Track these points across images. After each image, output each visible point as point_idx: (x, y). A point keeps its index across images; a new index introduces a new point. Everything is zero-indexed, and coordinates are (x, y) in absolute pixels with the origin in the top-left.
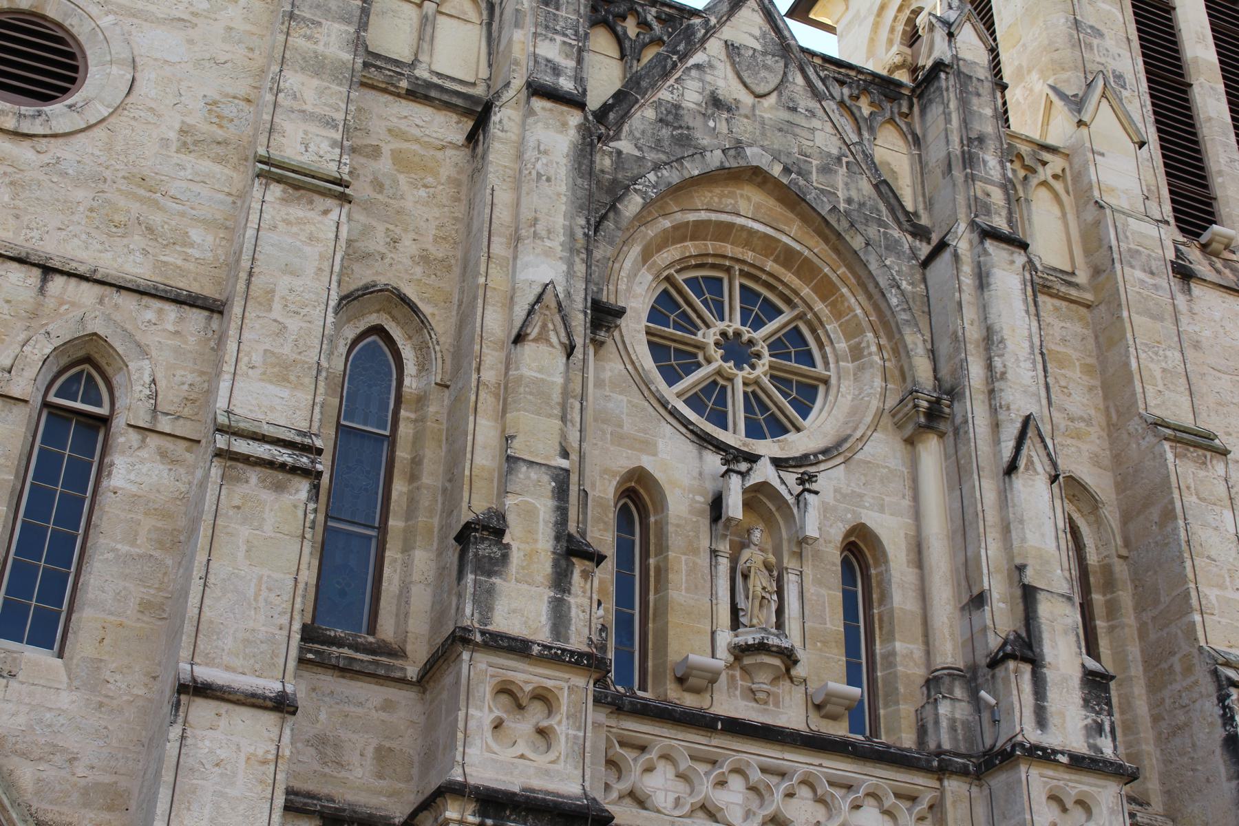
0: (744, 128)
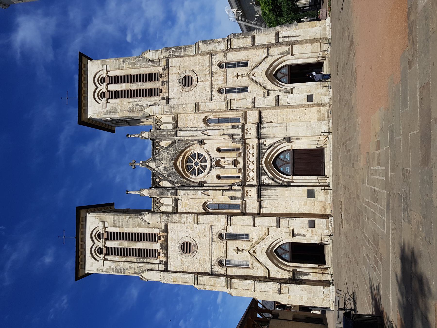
0: (168, 165)
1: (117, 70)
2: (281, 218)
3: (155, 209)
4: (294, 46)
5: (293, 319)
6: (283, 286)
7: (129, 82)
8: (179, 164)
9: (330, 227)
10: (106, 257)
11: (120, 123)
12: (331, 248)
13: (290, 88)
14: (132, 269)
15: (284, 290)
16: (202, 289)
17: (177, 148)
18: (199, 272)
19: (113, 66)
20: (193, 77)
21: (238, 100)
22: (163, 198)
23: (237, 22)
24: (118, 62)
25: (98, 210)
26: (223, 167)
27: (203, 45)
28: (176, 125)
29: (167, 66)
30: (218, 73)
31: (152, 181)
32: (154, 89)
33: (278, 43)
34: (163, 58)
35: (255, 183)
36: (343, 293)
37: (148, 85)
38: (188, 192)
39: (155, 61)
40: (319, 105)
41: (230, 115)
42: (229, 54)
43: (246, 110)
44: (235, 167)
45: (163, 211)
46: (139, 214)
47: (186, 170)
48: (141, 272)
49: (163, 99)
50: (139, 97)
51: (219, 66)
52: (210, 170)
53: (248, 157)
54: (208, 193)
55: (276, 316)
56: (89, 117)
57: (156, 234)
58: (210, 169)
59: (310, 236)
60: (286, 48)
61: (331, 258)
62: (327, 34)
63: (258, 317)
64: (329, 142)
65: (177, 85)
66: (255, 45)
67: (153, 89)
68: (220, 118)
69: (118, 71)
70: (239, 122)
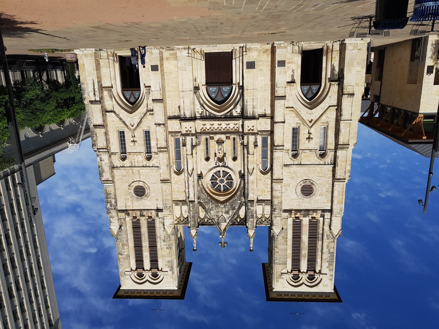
1: (130, 261)
2: (275, 94)
3: (267, 222)
4: (103, 86)
5: (379, 80)
6: (345, 91)
7: (142, 249)
8: (222, 199)
9: (284, 45)
10: (317, 271)
11: (182, 258)
12: (306, 43)
13: (145, 89)
14: (330, 245)
15: (349, 91)
16: (349, 174)
17: (206, 200)
18: (332, 177)
19: (126, 264)
20: (135, 186)
21: (158, 141)
22: (256, 214)
23: (80, 142)
24: (122, 260)
25: (270, 279)
26: (225, 154)
27: (104, 176)
28: (183, 202)
29: (125, 212)
30: (131, 161)
31: (240, 226)
32: (148, 224)
33: (100, 102)
34: (117, 215)
35: (240, 122)
36: (354, 30)
37: (144, 230)
38: (250, 189)
39: (121, 223)
40: (162, 59)
41: (172, 148)
42: (112, 151)
43: (168, 132)
44: (224, 143)
45: (270, 214)
46: (274, 239)
47: (228, 192)
48: (333, 236)
49: (157, 215)
50: (156, 239)
51: (124, 159)
52: (227, 167)
53: (214, 129)
54: (251, 169)
55: (377, 98)
56: (177, 289)
57: (294, 221)
58: (226, 168)
59: (294, 64)
60: (106, 93)
61: (316, 43)
62: (91, 52)
63: (378, 117)
64: (198, 48)
65: (143, 201)
66: (103, 124)
67: (148, 225)
68: (175, 158)
69: (130, 260)
70: (179, 139)
